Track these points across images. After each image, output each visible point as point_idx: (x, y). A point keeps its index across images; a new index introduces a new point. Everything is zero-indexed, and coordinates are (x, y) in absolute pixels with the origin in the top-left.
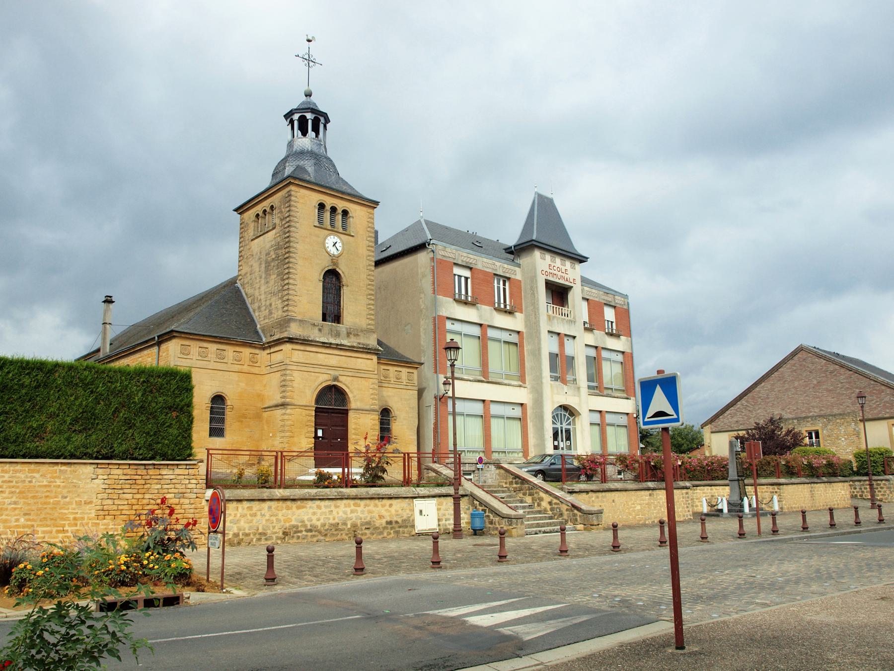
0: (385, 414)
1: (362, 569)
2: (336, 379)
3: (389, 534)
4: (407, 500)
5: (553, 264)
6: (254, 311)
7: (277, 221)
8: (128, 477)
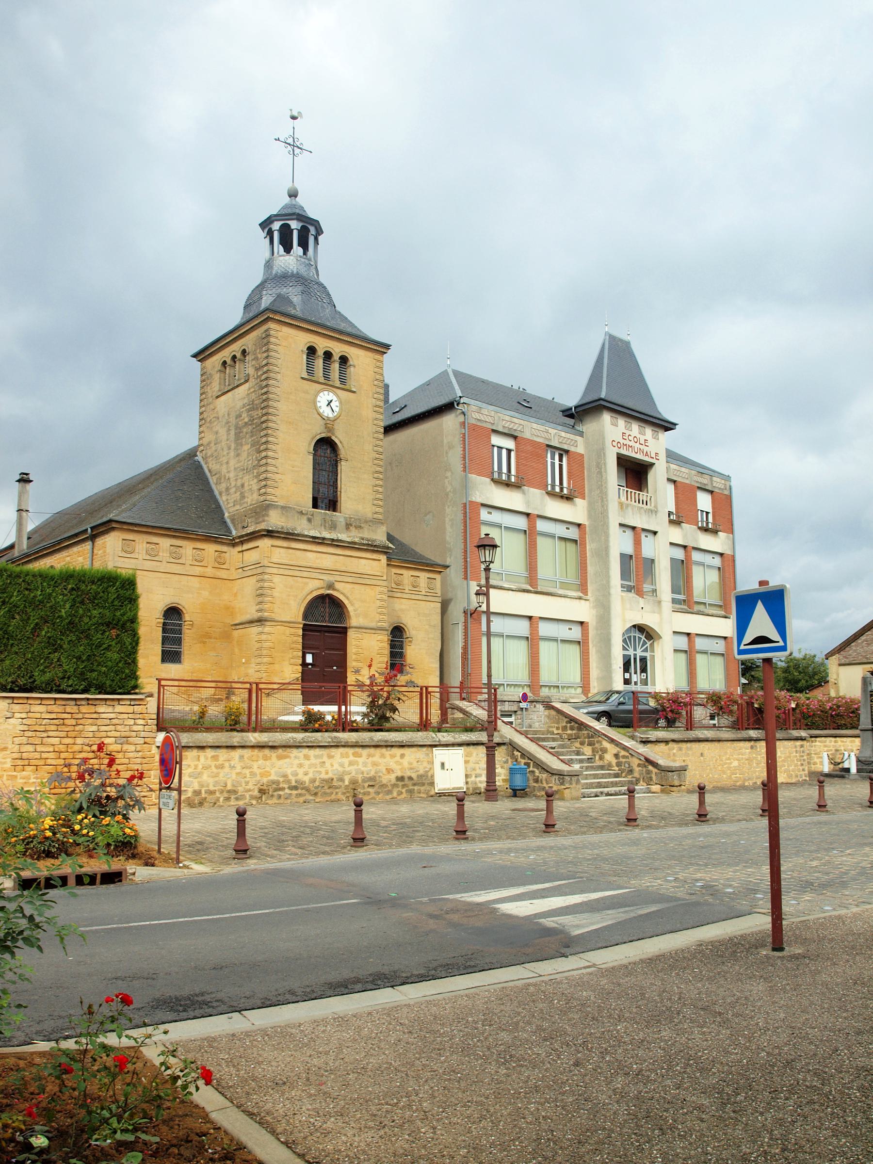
0: (397, 633)
1: (362, 839)
2: (331, 586)
3: (400, 793)
4: (424, 749)
5: (628, 433)
6: (220, 494)
7: (251, 371)
8: (53, 716)
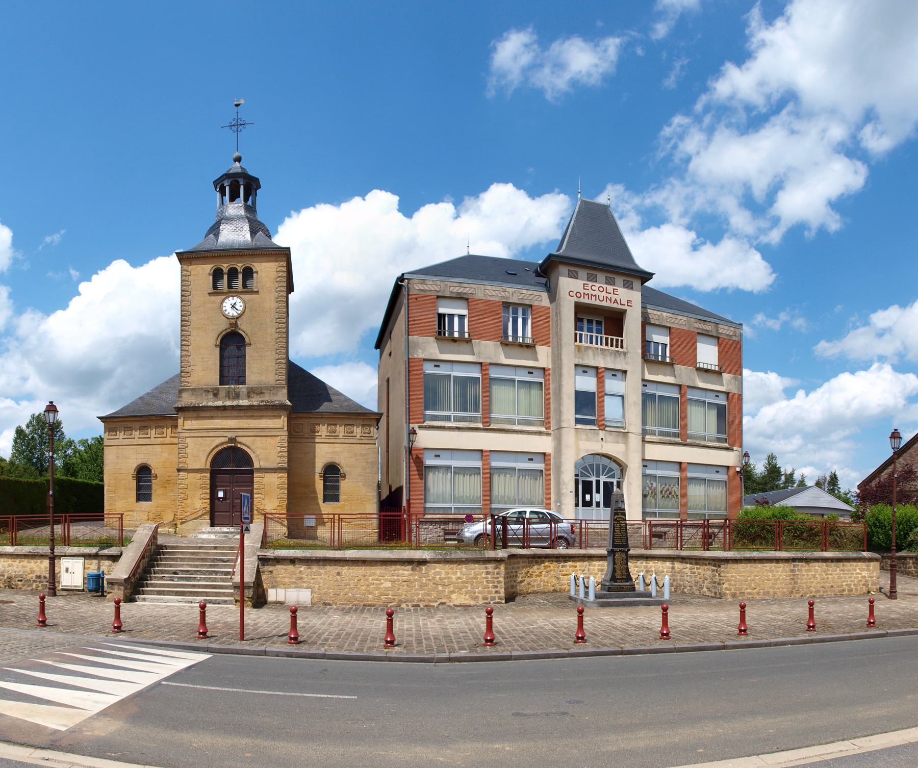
2: (232, 440)
